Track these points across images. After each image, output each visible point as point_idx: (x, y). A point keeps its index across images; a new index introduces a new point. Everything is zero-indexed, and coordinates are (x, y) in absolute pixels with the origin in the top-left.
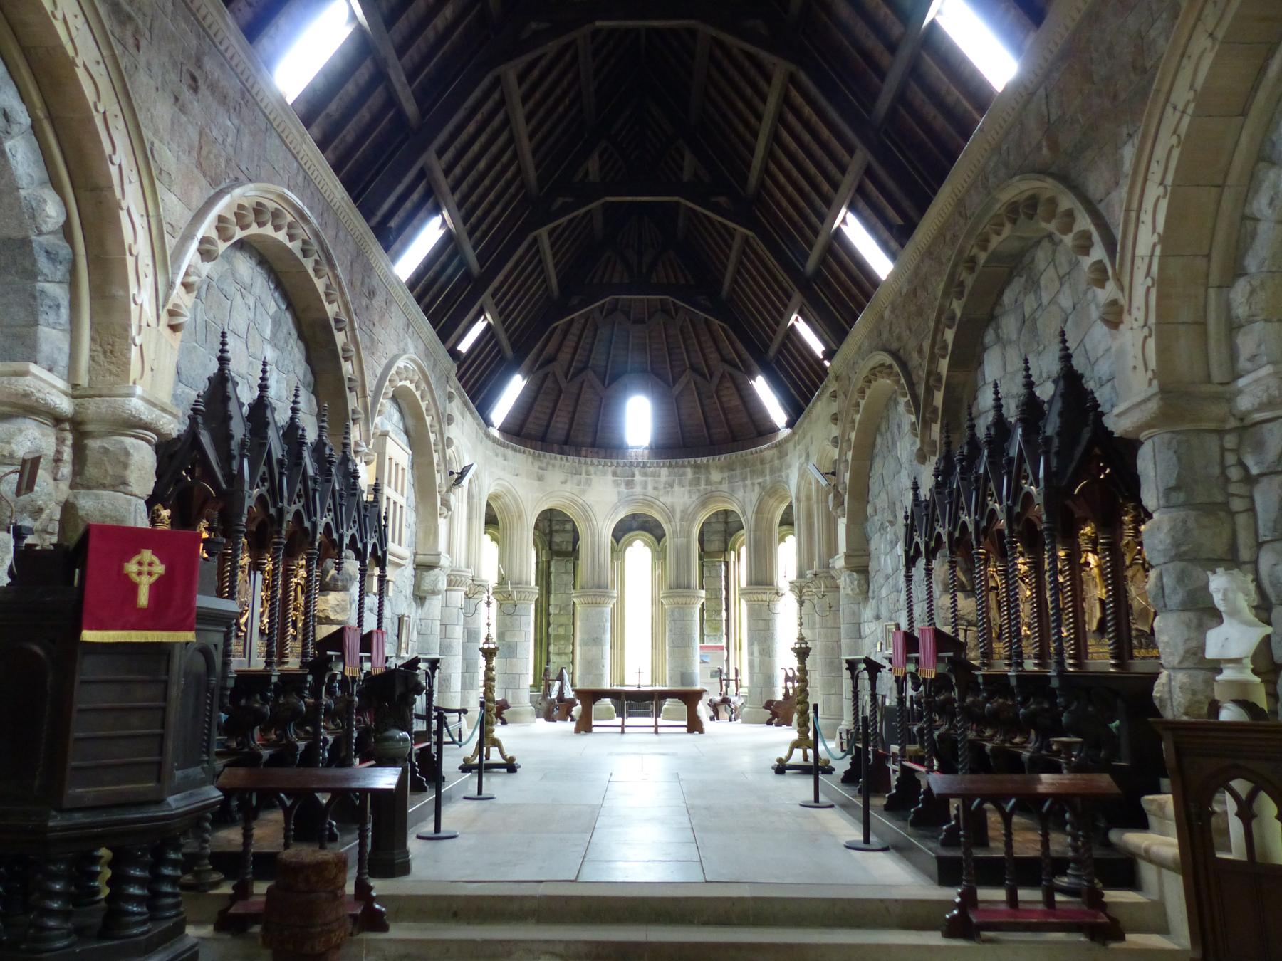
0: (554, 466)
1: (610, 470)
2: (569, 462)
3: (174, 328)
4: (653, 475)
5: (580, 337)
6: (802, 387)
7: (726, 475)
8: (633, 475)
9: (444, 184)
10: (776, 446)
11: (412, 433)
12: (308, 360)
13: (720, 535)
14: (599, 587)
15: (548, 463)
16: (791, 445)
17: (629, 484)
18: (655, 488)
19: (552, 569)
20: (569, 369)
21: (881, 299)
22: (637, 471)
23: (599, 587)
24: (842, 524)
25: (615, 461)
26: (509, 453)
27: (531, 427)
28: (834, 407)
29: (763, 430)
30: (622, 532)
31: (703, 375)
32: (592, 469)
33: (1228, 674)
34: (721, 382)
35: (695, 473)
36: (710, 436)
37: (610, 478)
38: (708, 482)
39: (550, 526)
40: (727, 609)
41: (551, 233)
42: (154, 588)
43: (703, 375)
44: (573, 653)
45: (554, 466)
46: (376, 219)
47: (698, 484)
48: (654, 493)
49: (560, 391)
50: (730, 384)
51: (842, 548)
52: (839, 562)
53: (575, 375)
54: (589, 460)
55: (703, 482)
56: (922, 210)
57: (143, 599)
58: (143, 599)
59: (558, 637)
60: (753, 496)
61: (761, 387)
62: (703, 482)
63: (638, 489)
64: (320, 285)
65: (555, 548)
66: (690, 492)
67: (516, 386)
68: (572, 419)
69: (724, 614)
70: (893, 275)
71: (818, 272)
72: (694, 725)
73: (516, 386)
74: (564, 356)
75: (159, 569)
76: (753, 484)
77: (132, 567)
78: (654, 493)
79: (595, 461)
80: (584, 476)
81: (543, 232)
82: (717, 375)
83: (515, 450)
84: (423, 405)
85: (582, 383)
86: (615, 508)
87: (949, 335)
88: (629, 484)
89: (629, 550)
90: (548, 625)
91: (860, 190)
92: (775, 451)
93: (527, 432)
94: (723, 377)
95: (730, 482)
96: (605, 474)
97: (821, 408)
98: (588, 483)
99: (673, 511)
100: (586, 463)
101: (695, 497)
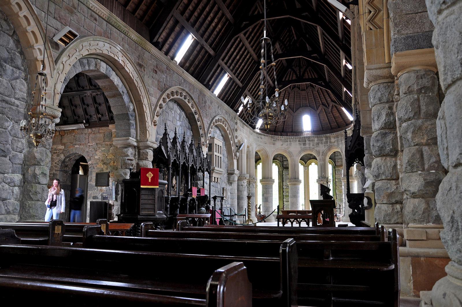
0: (278, 140)
3: (155, 125)
4: (312, 141)
8: (306, 141)
9: (226, 67)
11: (224, 136)
12: (189, 123)
14: (295, 179)
15: (276, 139)
17: (304, 144)
19: (284, 174)
23: (295, 179)
26: (263, 137)
31: (326, 106)
34: (332, 108)
35: (326, 139)
36: (331, 126)
37: (298, 142)
38: (330, 142)
39: (283, 159)
43: (326, 106)
45: (278, 140)
48: (313, 147)
50: (335, 109)
55: (329, 143)
57: (150, 181)
58: (150, 181)
62: (329, 143)
63: (307, 146)
64: (190, 105)
65: (284, 166)
75: (152, 175)
77: (148, 175)
78: (313, 147)
79: (292, 137)
80: (289, 142)
82: (331, 106)
83: (265, 135)
84: (226, 128)
86: (300, 152)
88: (304, 144)
89: (310, 166)
90: (283, 192)
94: (332, 106)
95: (337, 142)
96: (296, 141)
98: (290, 144)
101: (326, 147)
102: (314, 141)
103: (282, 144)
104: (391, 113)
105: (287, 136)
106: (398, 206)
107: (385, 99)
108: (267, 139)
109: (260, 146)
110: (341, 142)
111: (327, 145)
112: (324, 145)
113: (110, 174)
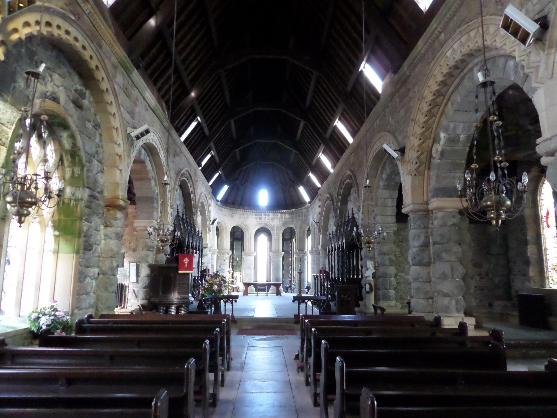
4: (268, 215)
6: (313, 192)
16: (310, 209)
17: (260, 218)
21: (330, 178)
22: (263, 214)
24: (321, 236)
26: (223, 209)
27: (230, 200)
28: (320, 203)
33: (368, 279)
37: (254, 216)
40: (291, 257)
41: (239, 150)
46: (175, 124)
51: (321, 244)
52: (320, 247)
56: (341, 155)
57: (186, 266)
58: (186, 266)
60: (299, 224)
63: (263, 220)
64: (189, 185)
65: (235, 237)
67: (225, 188)
70: (353, 142)
72: (279, 293)
73: (225, 188)
81: (237, 151)
86: (256, 226)
87: (340, 197)
88: (260, 218)
91: (324, 150)
93: (228, 202)
96: (252, 215)
97: (317, 203)
98: (247, 217)
99: (274, 227)
101: (281, 223)
104: (427, 237)
106: (431, 301)
107: (422, 226)
108: (226, 211)
113: (125, 255)
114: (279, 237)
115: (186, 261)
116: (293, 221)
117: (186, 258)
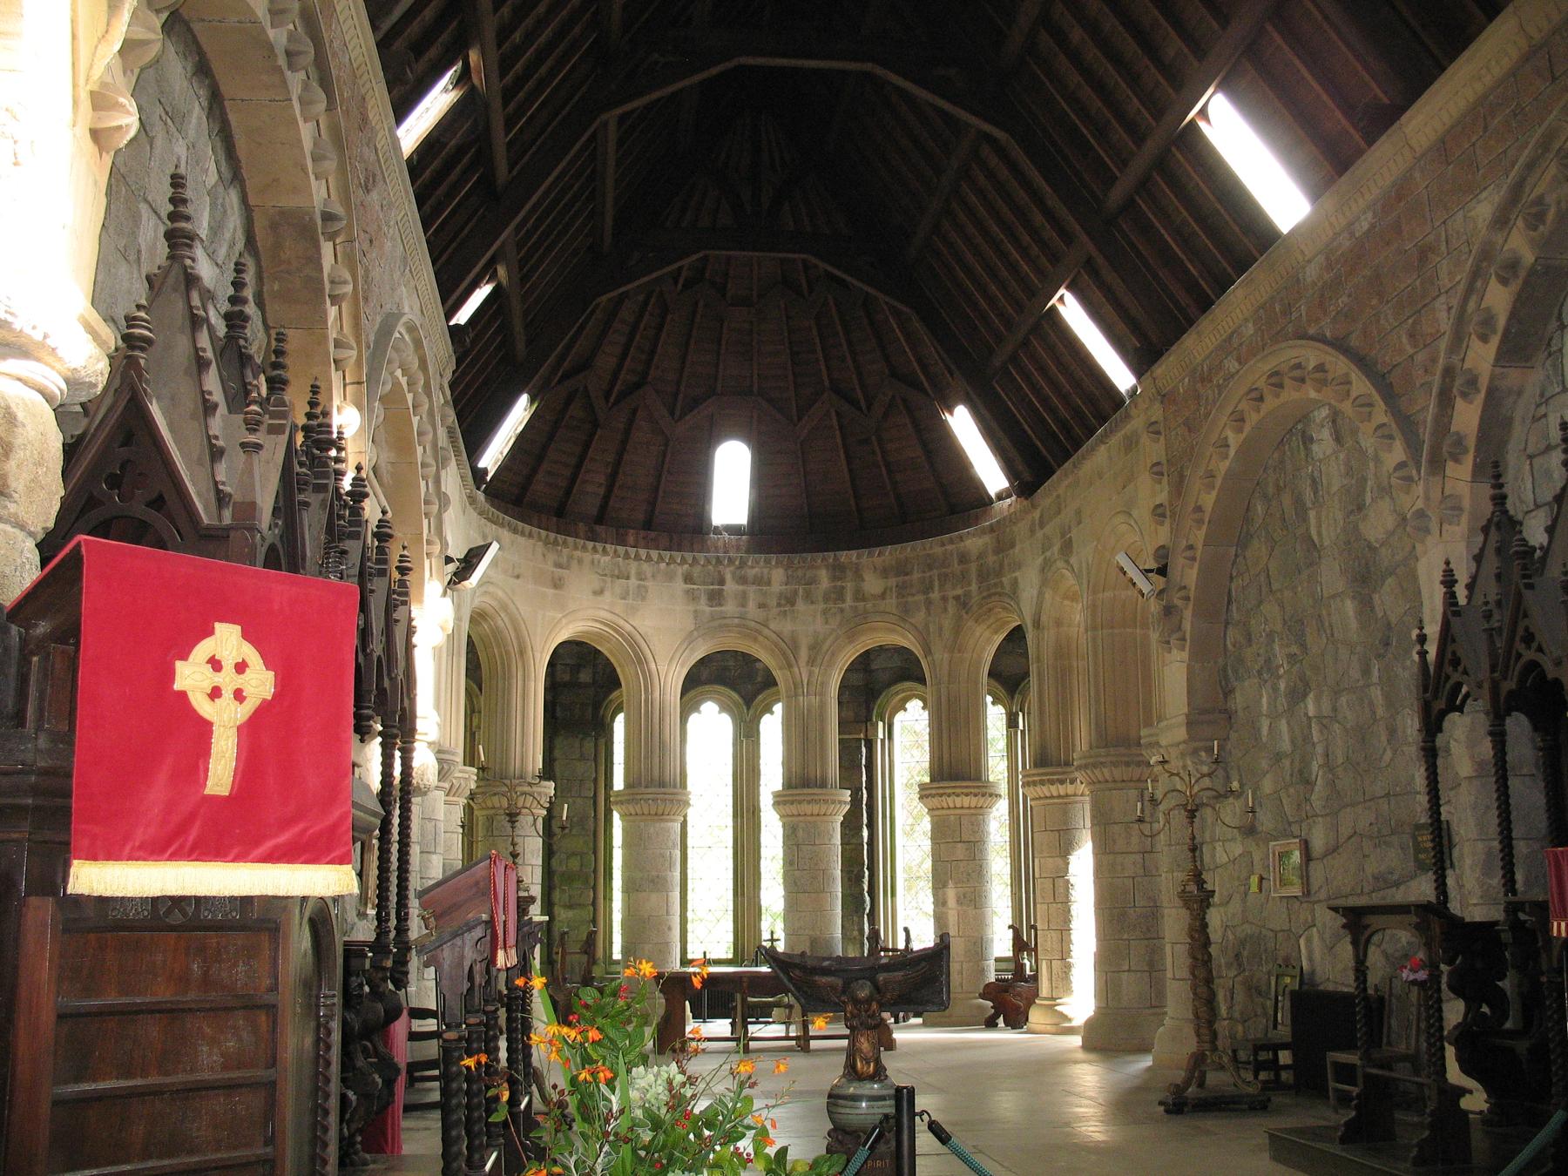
0: (580, 561)
1: (681, 571)
2: (606, 557)
4: (760, 581)
5: (634, 328)
7: (892, 582)
8: (722, 582)
10: (992, 529)
13: (869, 691)
15: (570, 558)
16: (1022, 528)
17: (716, 598)
18: (762, 606)
20: (612, 384)
23: (662, 784)
25: (689, 556)
29: (966, 500)
30: (699, 681)
32: (645, 567)
35: (834, 578)
37: (679, 586)
38: (859, 596)
40: (871, 826)
42: (251, 731)
43: (854, 403)
44: (594, 904)
47: (840, 595)
49: (595, 425)
53: (623, 395)
54: (643, 553)
57: (221, 772)
59: (570, 878)
61: (962, 424)
63: (730, 607)
66: (825, 612)
68: (613, 477)
69: (865, 833)
71: (1129, 205)
74: (606, 361)
75: (261, 683)
76: (944, 599)
77: (190, 676)
79: (654, 554)
80: (633, 582)
83: (515, 531)
85: (635, 411)
88: (716, 598)
92: (987, 539)
95: (900, 595)
96: (670, 577)
98: (642, 594)
99: (795, 647)
100: (637, 558)
102: (769, 583)
103: (597, 586)
105: (623, 543)
109: (491, 589)
110: (920, 597)
111: (842, 610)
112: (822, 606)
114: (823, 706)
115: (224, 677)
116: (905, 611)
117: (227, 640)
